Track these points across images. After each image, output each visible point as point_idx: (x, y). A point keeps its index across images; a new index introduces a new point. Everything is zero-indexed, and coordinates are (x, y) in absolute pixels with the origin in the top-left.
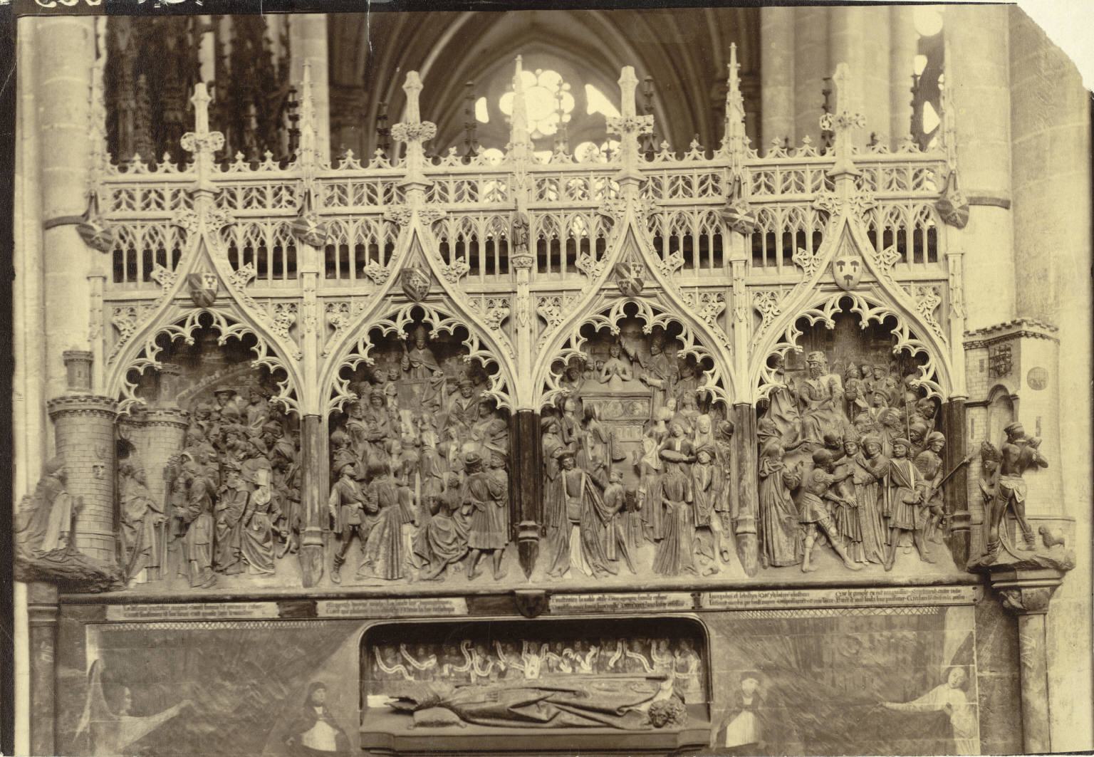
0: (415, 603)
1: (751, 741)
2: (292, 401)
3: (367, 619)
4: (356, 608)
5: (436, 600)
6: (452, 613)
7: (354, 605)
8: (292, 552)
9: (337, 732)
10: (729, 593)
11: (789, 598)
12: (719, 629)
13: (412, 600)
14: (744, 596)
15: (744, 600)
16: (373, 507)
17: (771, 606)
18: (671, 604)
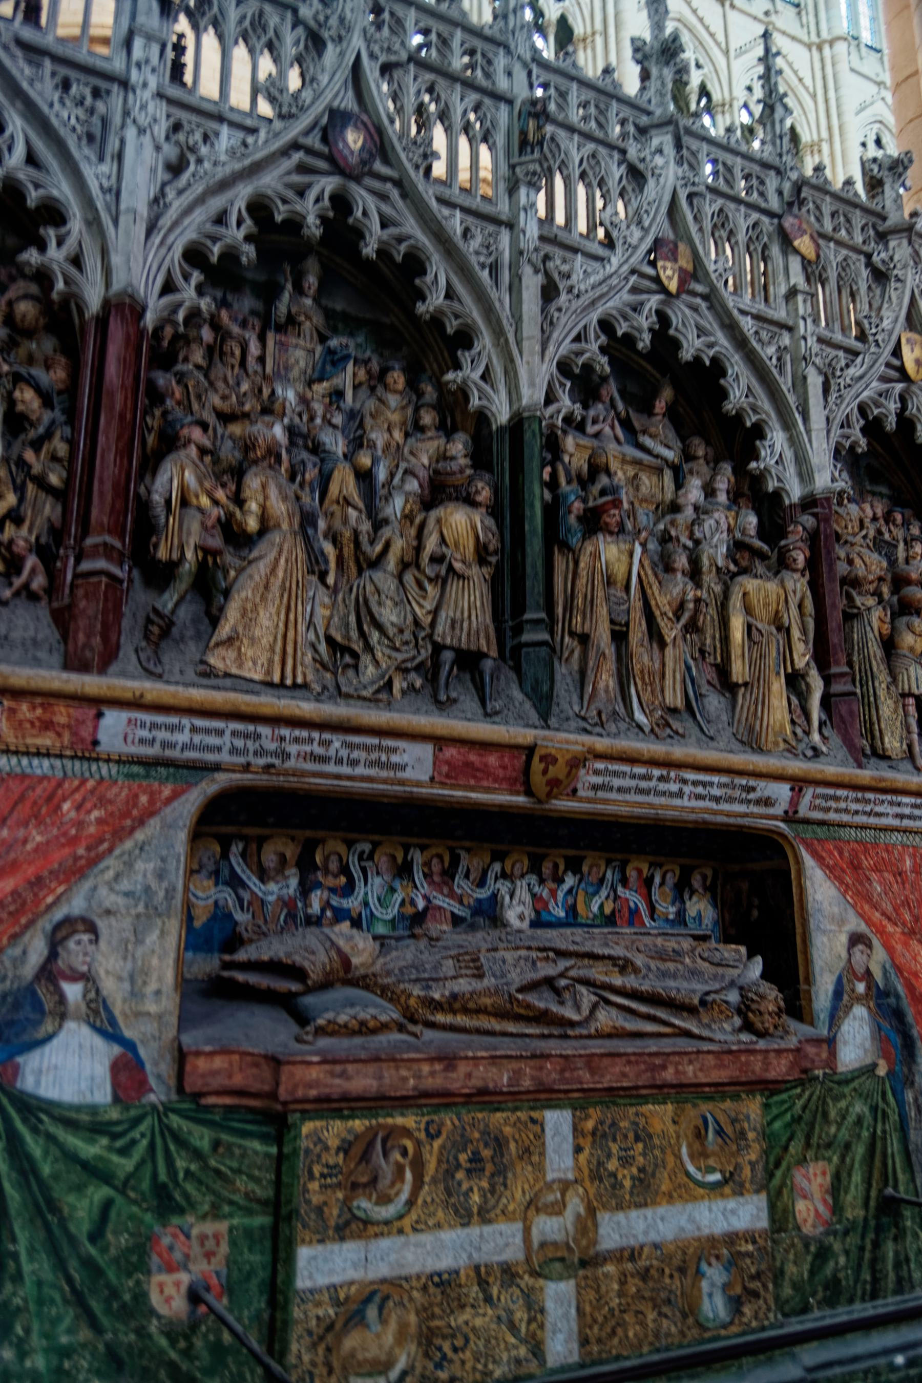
0: (328, 743)
1: (868, 1061)
2: (73, 271)
3: (217, 767)
4: (197, 739)
5: (375, 741)
6: (400, 775)
7: (194, 730)
8: (33, 597)
9: (117, 1050)
10: (840, 793)
11: (907, 811)
12: (815, 855)
13: (327, 736)
14: (857, 800)
15: (854, 807)
16: (252, 524)
17: (884, 821)
18: (758, 802)
